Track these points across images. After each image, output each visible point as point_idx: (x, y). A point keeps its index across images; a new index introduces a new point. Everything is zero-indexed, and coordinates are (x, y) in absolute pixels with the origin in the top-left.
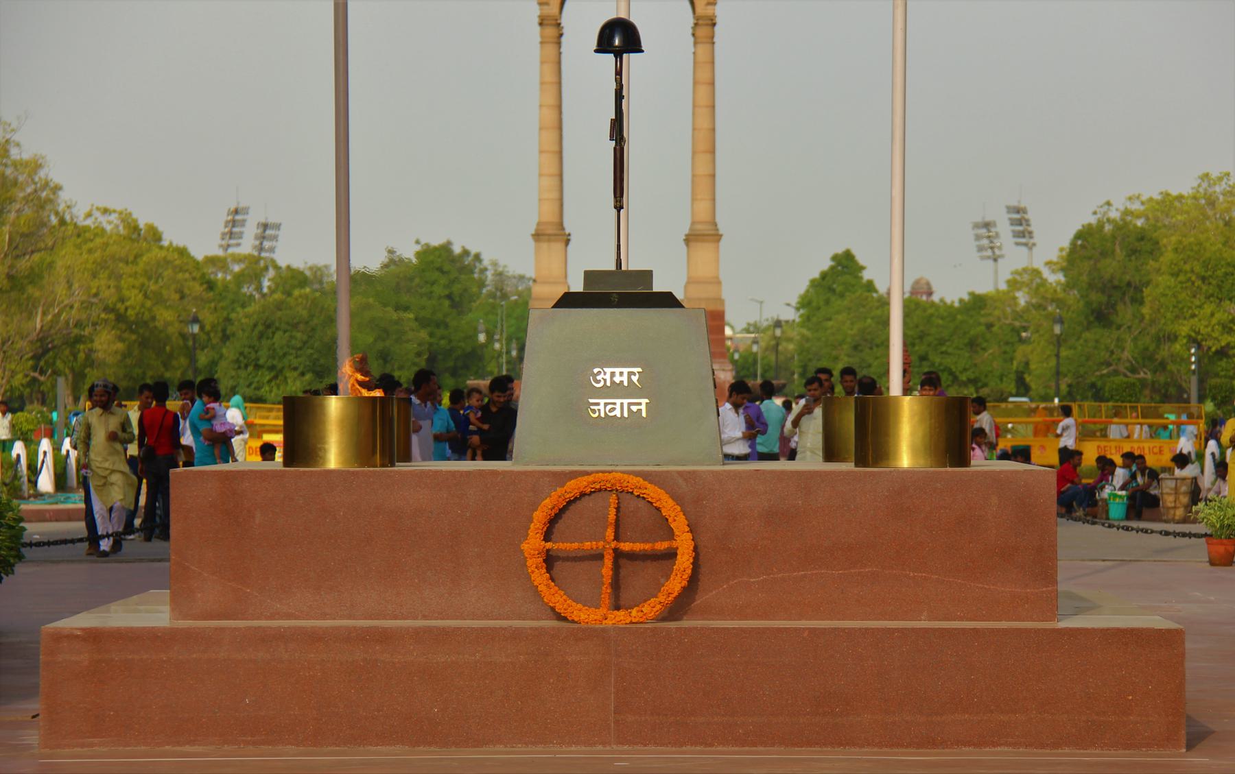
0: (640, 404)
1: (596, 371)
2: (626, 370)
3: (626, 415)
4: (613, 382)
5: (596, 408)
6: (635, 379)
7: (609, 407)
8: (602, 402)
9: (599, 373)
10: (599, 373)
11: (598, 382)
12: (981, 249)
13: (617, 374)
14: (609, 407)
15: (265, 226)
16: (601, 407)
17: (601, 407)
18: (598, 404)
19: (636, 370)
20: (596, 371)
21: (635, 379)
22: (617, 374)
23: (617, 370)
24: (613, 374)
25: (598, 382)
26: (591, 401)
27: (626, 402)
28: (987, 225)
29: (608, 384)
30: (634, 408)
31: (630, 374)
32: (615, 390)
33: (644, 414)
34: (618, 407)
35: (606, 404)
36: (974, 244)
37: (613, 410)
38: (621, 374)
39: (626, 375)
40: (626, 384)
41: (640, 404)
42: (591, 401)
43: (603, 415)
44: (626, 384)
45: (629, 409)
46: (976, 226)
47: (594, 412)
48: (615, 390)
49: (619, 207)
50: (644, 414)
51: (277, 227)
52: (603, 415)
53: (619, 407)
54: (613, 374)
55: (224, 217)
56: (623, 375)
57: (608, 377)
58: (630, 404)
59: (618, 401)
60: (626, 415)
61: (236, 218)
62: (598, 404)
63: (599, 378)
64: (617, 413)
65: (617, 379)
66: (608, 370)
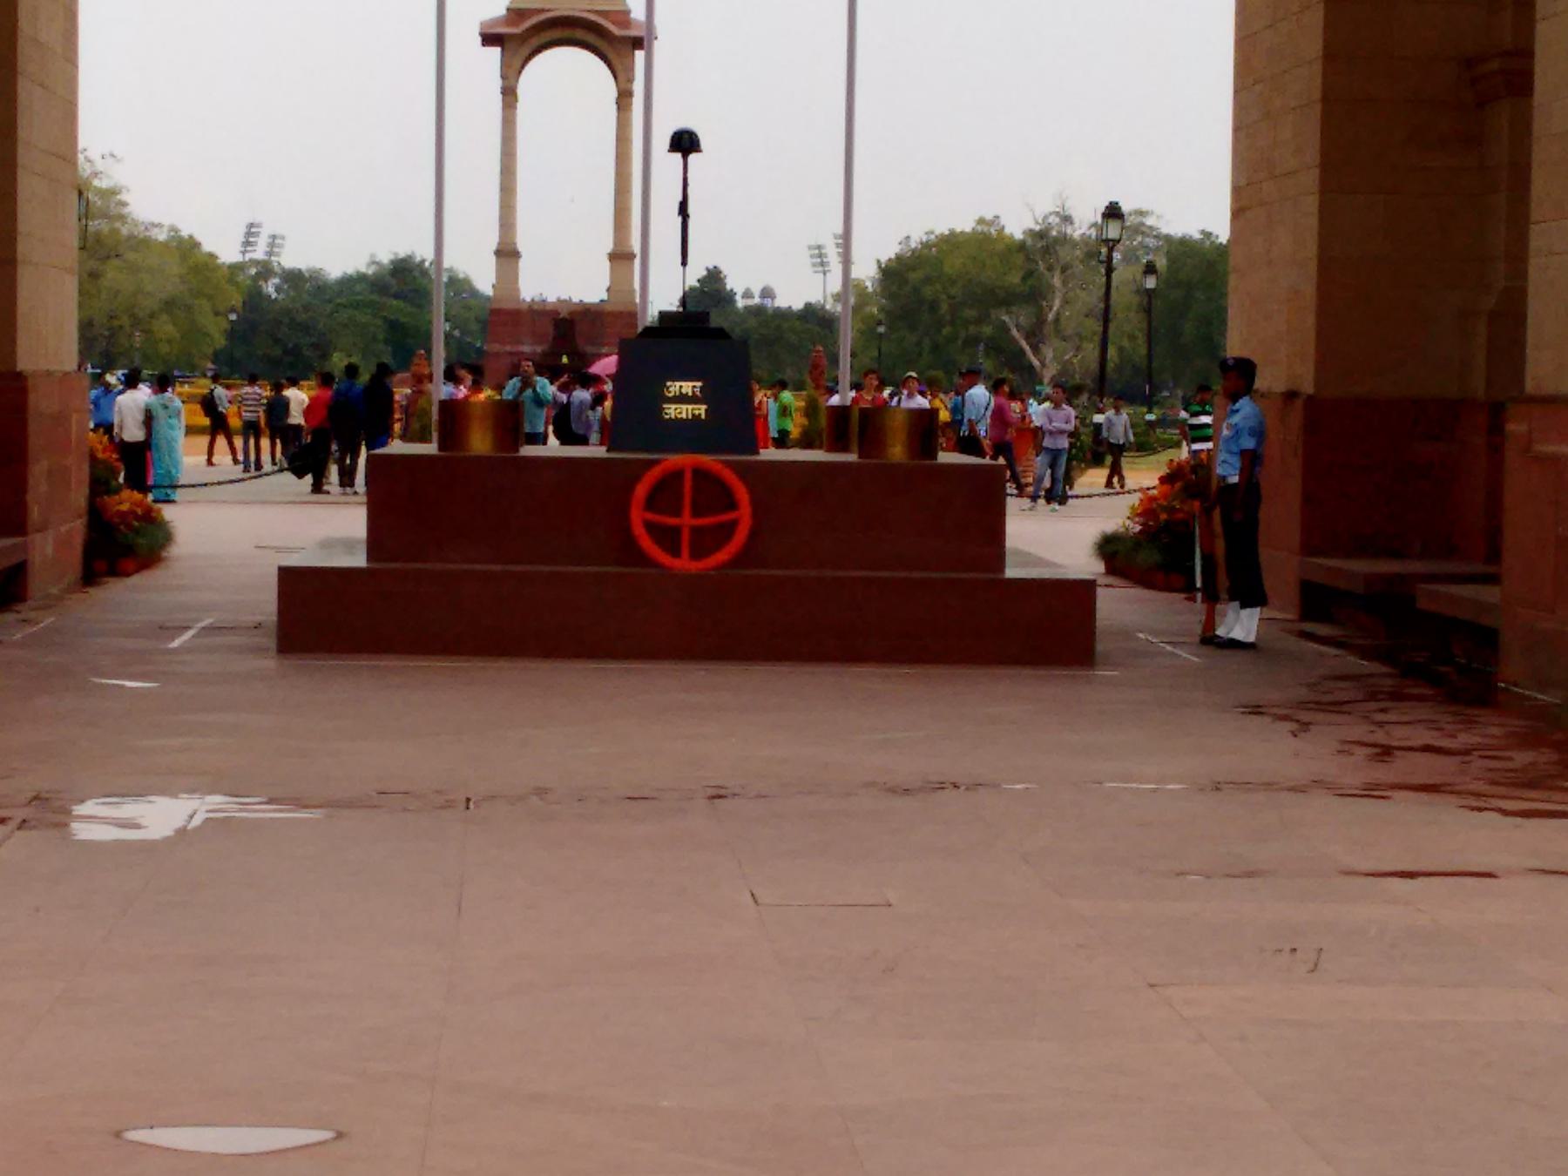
12: (814, 265)
15: (274, 237)
16: (672, 411)
19: (699, 384)
28: (819, 247)
32: (682, 399)
36: (808, 261)
46: (810, 248)
48: (682, 399)
49: (684, 263)
51: (283, 238)
53: (683, 411)
55: (243, 230)
56: (687, 387)
59: (684, 407)
61: (251, 232)
66: (678, 384)
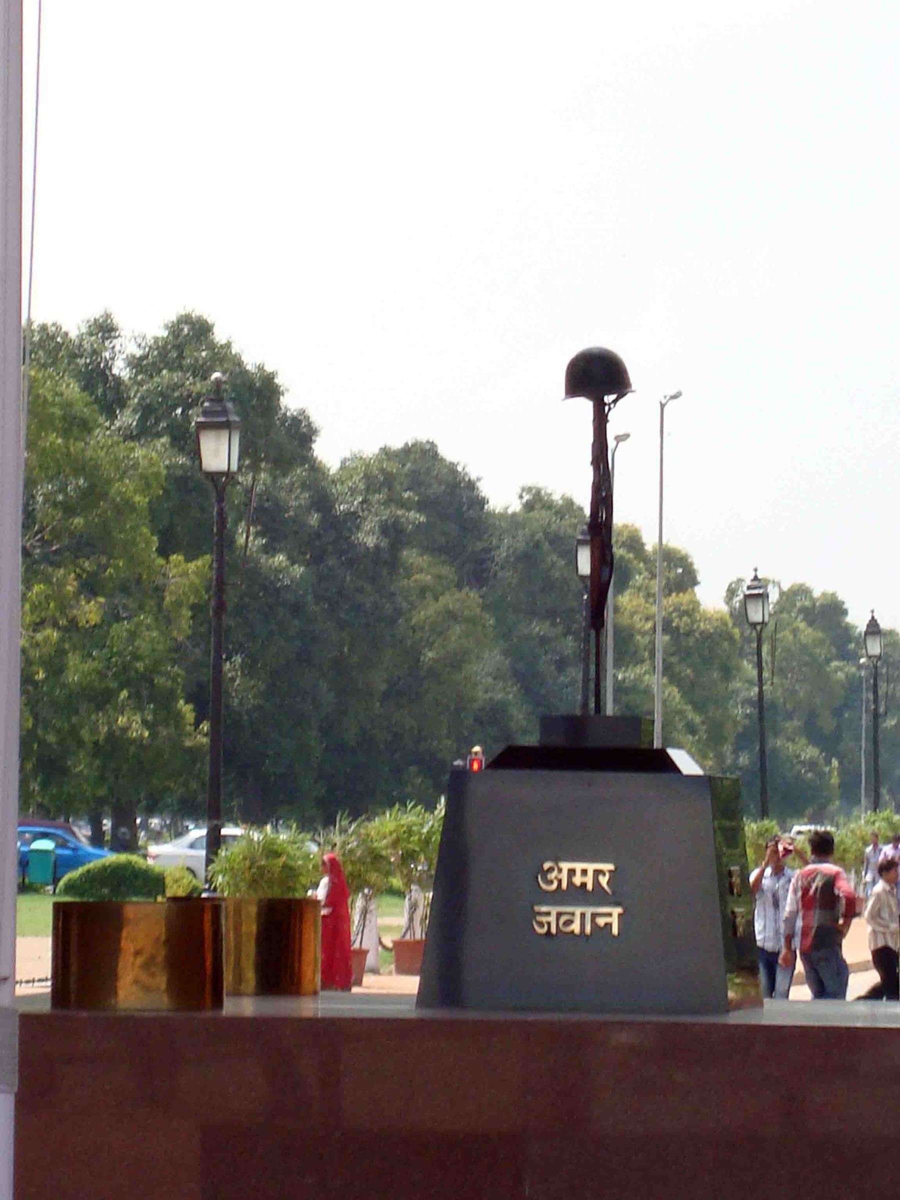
0: (610, 915)
1: (547, 865)
2: (591, 867)
3: (588, 929)
4: (570, 883)
5: (544, 919)
6: (604, 881)
7: (563, 919)
8: (554, 910)
9: (551, 870)
10: (551, 870)
11: (552, 882)
13: (578, 873)
14: (563, 919)
16: (549, 917)
17: (552, 919)
18: (548, 914)
20: (547, 865)
21: (604, 881)
22: (578, 873)
23: (579, 866)
24: (572, 872)
26: (537, 908)
27: (589, 911)
29: (564, 885)
30: (601, 921)
31: (597, 873)
33: (615, 931)
35: (559, 915)
37: (569, 922)
38: (584, 872)
39: (590, 873)
40: (590, 887)
41: (610, 915)
42: (537, 908)
43: (554, 930)
44: (590, 887)
47: (541, 924)
50: (615, 931)
52: (554, 930)
53: (579, 919)
54: (572, 872)
56: (587, 871)
57: (564, 876)
58: (594, 916)
59: (578, 911)
60: (588, 929)
62: (548, 914)
63: (552, 876)
64: (576, 927)
65: (578, 880)
66: (565, 866)
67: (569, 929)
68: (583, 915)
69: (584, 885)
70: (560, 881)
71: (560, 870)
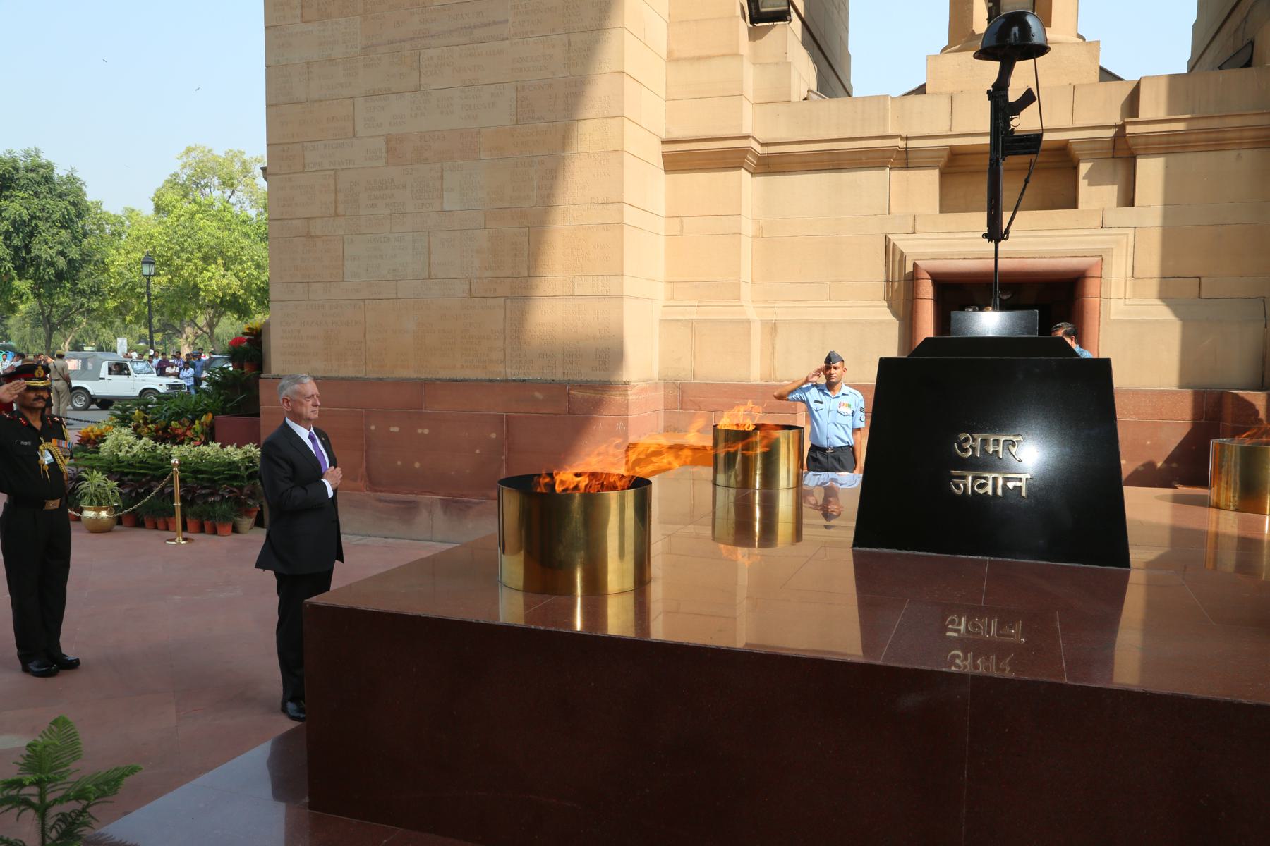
0: (1020, 480)
1: (963, 436)
3: (1000, 492)
4: (984, 451)
10: (966, 440)
11: (966, 451)
25: (966, 451)
30: (1011, 485)
33: (1024, 494)
34: (990, 482)
35: (975, 478)
37: (982, 486)
38: (996, 442)
45: (1005, 486)
50: (1024, 494)
54: (985, 442)
60: (1000, 492)
66: (979, 437)
67: (981, 491)
68: (995, 479)
69: (997, 452)
70: (974, 449)
71: (974, 440)
